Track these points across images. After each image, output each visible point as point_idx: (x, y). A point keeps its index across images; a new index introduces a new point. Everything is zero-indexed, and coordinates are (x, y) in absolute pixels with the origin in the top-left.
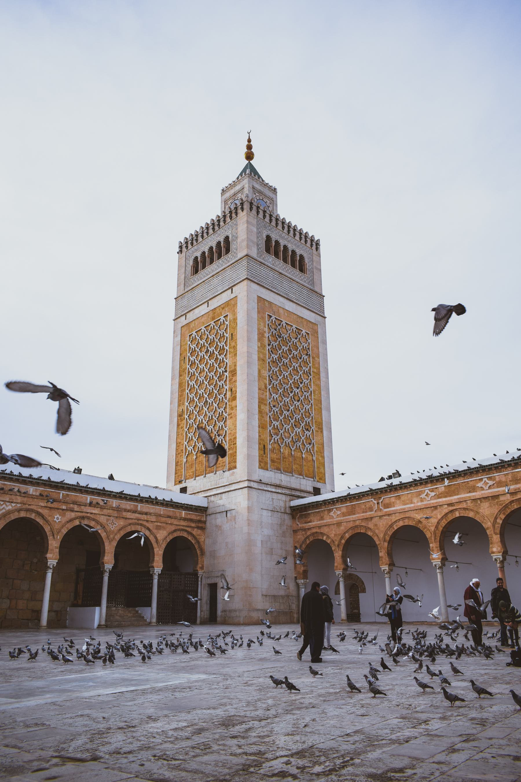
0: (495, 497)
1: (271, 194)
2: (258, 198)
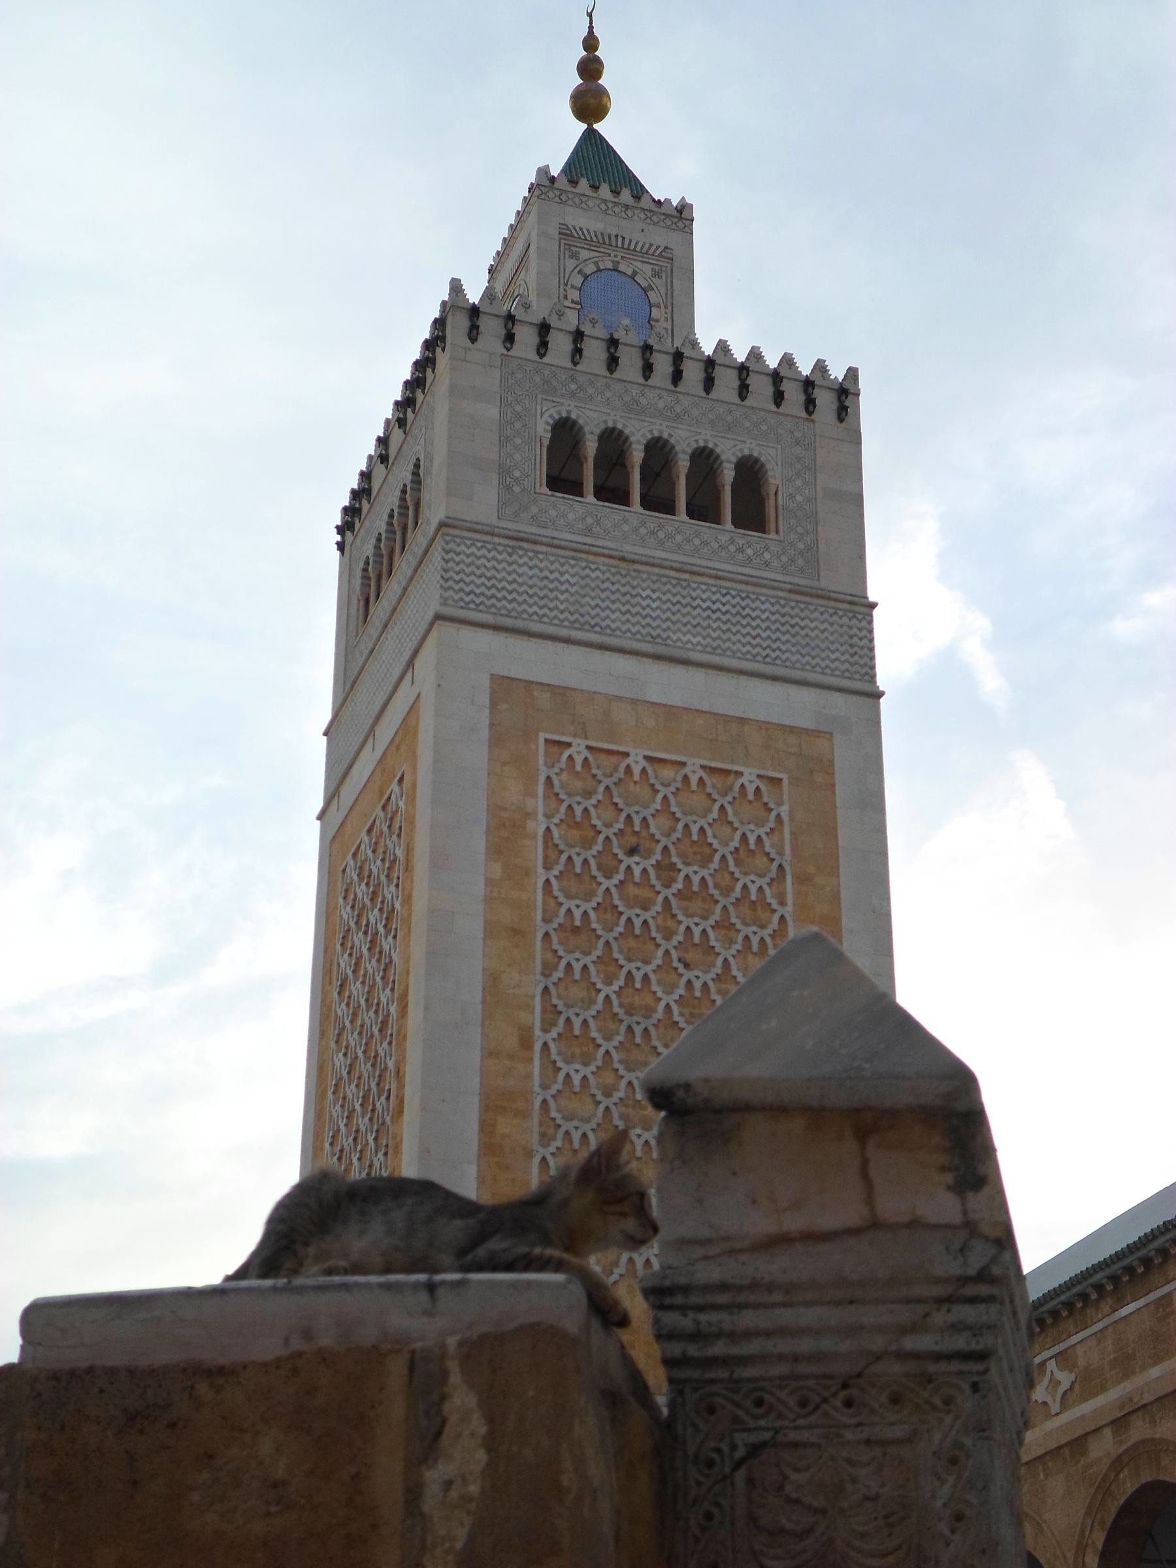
0: (1078, 1444)
1: (659, 237)
2: (590, 269)
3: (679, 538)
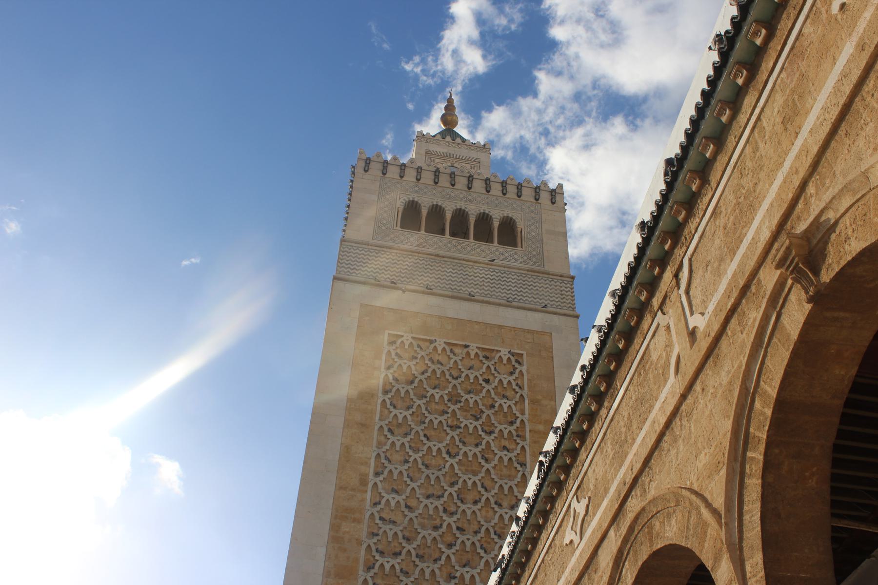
1: (474, 154)
3: (469, 249)
